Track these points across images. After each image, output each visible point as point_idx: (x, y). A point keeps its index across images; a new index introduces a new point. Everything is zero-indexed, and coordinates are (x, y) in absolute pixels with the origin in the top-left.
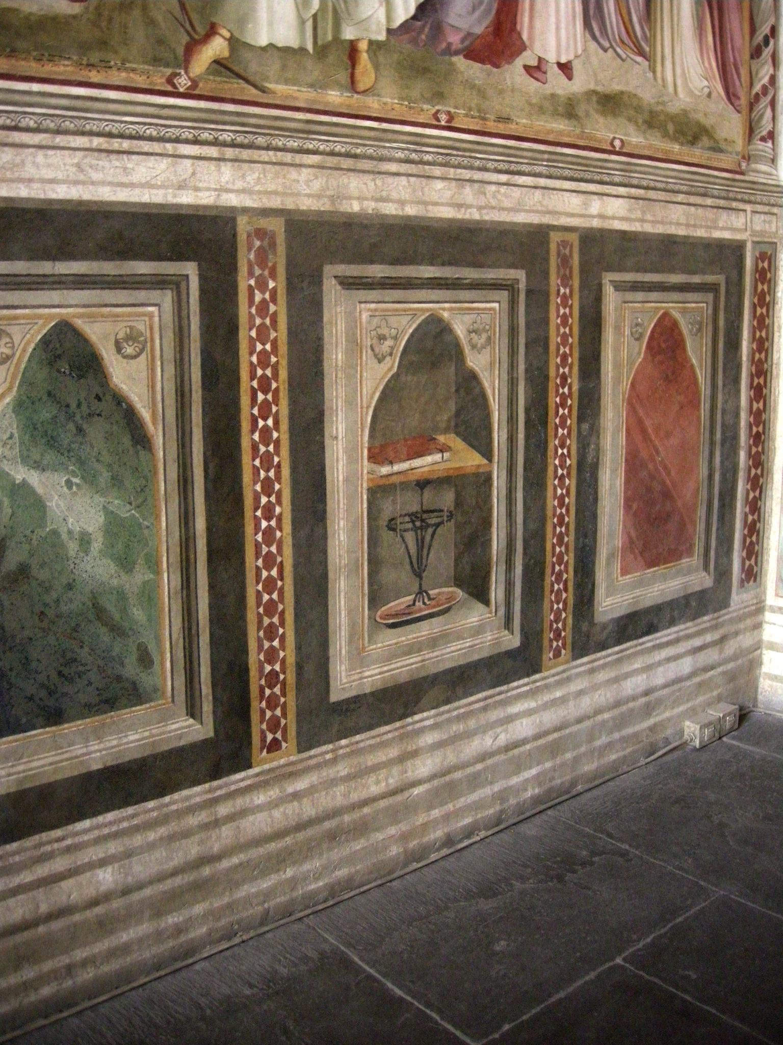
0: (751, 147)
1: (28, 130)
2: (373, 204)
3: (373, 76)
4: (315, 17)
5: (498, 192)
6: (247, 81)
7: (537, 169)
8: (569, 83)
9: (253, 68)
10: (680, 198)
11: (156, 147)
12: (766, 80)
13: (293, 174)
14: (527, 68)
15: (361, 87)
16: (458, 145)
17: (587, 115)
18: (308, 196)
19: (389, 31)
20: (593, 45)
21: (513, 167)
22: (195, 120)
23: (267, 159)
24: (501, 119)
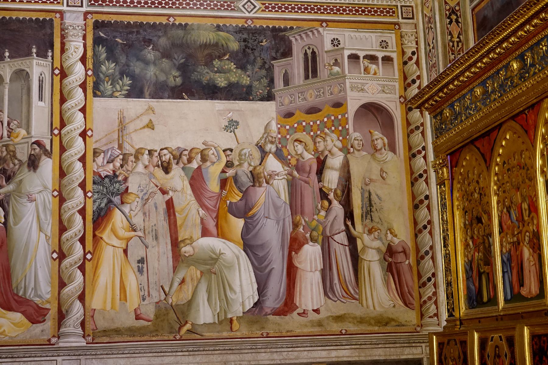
0: (423, 321)
4: (218, 313)
6: (197, 334)
7: (305, 345)
9: (199, 330)
11: (170, 354)
12: (430, 294)
13: (212, 357)
14: (298, 314)
15: (234, 330)
16: (271, 342)
17: (328, 324)
18: (217, 362)
19: (243, 313)
20: (329, 301)
21: (294, 346)
22: (182, 346)
23: (203, 353)
24: (288, 331)
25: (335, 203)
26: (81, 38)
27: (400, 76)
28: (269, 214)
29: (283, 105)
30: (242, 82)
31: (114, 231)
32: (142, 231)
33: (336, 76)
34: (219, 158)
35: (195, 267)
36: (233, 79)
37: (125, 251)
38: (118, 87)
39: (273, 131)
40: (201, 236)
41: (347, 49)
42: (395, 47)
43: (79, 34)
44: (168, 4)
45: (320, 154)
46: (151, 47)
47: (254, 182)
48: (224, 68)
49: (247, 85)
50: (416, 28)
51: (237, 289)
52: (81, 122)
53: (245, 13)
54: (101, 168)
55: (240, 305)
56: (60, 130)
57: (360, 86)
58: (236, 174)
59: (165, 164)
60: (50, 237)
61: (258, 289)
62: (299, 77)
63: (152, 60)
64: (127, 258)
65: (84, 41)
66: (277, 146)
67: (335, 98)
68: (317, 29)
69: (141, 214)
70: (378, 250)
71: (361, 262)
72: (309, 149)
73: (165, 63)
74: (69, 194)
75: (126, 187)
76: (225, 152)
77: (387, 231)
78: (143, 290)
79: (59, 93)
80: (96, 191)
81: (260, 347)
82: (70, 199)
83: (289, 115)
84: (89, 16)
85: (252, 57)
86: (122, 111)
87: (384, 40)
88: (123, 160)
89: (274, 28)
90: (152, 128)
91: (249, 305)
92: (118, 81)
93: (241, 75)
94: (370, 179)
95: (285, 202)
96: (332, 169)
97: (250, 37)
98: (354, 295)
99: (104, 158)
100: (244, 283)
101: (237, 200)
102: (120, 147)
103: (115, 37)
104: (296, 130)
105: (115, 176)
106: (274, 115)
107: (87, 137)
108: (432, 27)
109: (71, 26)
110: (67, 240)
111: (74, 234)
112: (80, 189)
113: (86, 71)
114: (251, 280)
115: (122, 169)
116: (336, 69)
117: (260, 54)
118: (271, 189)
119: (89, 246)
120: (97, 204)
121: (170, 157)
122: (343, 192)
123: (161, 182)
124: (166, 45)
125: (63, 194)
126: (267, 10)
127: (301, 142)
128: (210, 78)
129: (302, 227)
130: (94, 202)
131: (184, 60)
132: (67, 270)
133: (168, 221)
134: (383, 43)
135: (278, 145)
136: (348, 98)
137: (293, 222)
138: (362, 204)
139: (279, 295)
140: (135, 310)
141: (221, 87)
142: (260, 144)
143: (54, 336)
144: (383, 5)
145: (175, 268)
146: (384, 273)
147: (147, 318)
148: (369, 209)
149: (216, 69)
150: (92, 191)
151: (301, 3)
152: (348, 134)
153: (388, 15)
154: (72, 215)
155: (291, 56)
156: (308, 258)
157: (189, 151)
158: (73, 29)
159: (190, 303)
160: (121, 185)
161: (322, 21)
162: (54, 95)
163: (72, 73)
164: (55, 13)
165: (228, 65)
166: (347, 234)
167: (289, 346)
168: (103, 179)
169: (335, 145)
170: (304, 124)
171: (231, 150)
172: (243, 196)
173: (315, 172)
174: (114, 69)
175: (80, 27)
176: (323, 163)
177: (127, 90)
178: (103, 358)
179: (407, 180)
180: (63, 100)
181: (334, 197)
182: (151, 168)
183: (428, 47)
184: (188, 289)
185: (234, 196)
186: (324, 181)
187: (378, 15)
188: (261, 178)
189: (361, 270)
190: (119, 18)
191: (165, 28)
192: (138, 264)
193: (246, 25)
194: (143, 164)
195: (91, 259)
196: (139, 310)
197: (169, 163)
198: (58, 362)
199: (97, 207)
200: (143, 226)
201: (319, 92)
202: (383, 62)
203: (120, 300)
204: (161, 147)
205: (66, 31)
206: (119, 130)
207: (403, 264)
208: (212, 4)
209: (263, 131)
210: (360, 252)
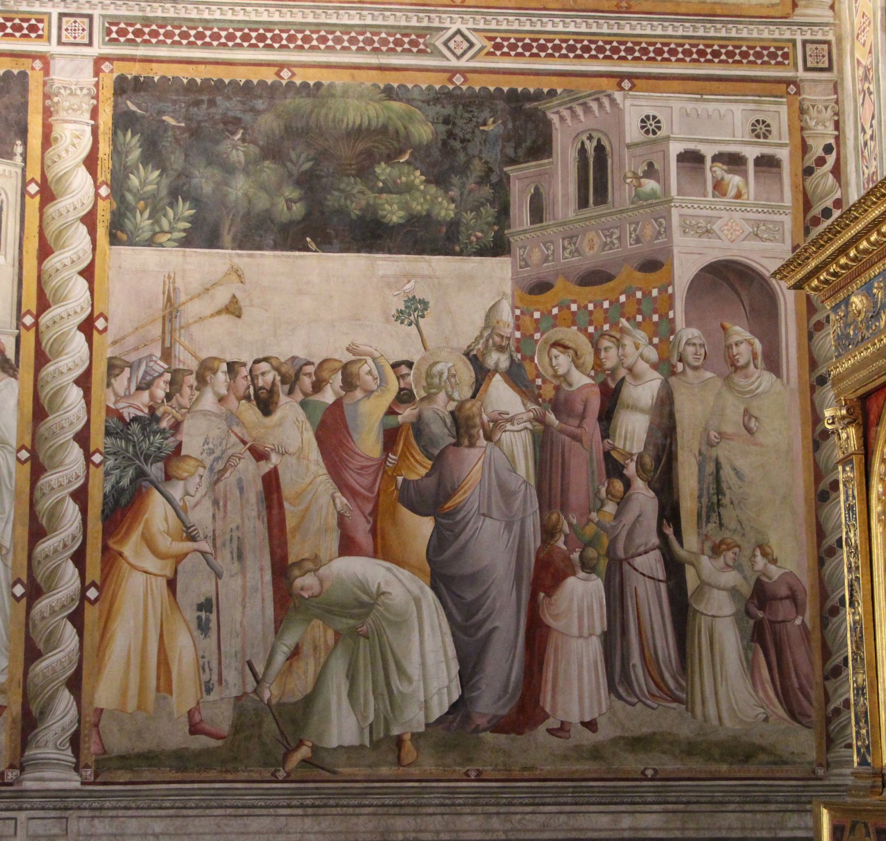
1: (191, 808)
2: (414, 835)
3: (415, 754)
4: (371, 726)
5: (524, 819)
8: (594, 735)
10: (731, 807)
11: (264, 811)
13: (354, 820)
14: (551, 731)
15: (406, 762)
17: (614, 754)
18: (364, 832)
19: (427, 725)
20: (619, 704)
21: (537, 801)
22: (289, 795)
24: (524, 769)
25: (639, 485)
26: (87, 117)
27: (795, 199)
28: (489, 507)
29: (527, 265)
30: (439, 214)
31: (148, 541)
32: (210, 541)
33: (650, 202)
34: (382, 380)
35: (324, 622)
36: (419, 207)
37: (172, 584)
38: (165, 223)
39: (504, 323)
40: (337, 554)
41: (676, 139)
42: (787, 136)
43: (84, 105)
44: (278, 40)
45: (608, 375)
46: (239, 136)
47: (458, 436)
48: (399, 181)
49: (448, 219)
50: (836, 92)
51: (414, 669)
52: (82, 299)
53: (448, 60)
54: (124, 400)
55: (421, 709)
56: (37, 317)
57: (702, 223)
58: (420, 417)
59: (263, 394)
60: (8, 551)
61: (461, 674)
62: (566, 204)
63: (240, 162)
64: (175, 599)
65: (92, 122)
66: (511, 356)
67: (645, 250)
68: (609, 96)
69: (207, 503)
70: (734, 592)
71: (694, 616)
72: (583, 364)
73: (269, 171)
74: (52, 457)
75: (177, 443)
76: (397, 369)
77: (754, 550)
78: (207, 670)
79: (37, 235)
80: (112, 450)
81: (461, 801)
82: (54, 468)
83: (541, 287)
84: (106, 67)
85: (462, 158)
86: (172, 275)
87: (761, 119)
88: (171, 383)
89: (513, 91)
90: (237, 313)
91: (439, 708)
92: (165, 209)
93: (436, 198)
94: (720, 433)
95: (526, 482)
96: (634, 408)
97: (459, 113)
98: (677, 693)
99: (130, 380)
100: (430, 658)
101: (418, 474)
102: (167, 355)
103: (161, 113)
104: (555, 322)
105: (154, 417)
106: (508, 288)
107: (95, 334)
108: (872, 89)
109: (65, 88)
110: (47, 556)
111: (61, 546)
112: (76, 446)
113: (97, 187)
114: (446, 655)
115: (170, 403)
116: (650, 185)
117: (481, 151)
118: (497, 452)
119: (94, 572)
120: (113, 479)
121: (274, 379)
122: (658, 459)
123: (254, 434)
124: (272, 130)
125: (41, 457)
126: (498, 53)
127: (566, 347)
128: (368, 204)
129: (563, 538)
130: (107, 474)
131: (310, 164)
132: (45, 622)
133: (266, 519)
134: (758, 127)
135: (514, 354)
136: (675, 251)
137: (541, 526)
138: (701, 489)
139: (506, 687)
140: (190, 713)
141: (391, 224)
142: (475, 352)
143: (12, 767)
144: (762, 40)
145: (280, 624)
146: (745, 643)
147: (213, 730)
148: (715, 500)
149: (381, 184)
150: (103, 451)
151: (575, 37)
152: (672, 331)
153: (773, 62)
154: (58, 502)
155: (550, 155)
156: (575, 607)
157: (316, 365)
158: (71, 94)
159: (309, 701)
160: (166, 439)
161: (621, 77)
162: (25, 239)
163: (65, 191)
164: (31, 60)
165: (408, 175)
166: (663, 555)
167: (526, 801)
168: (127, 425)
169: (641, 356)
170: (574, 307)
171: (410, 365)
172: (433, 466)
173: (597, 416)
174: (158, 184)
175: (85, 91)
176: (613, 395)
177: (185, 230)
178: (118, 817)
179: (804, 437)
180: (45, 251)
181: (637, 471)
182: (233, 403)
183: (861, 136)
184: (308, 668)
185: (415, 467)
186: (615, 436)
187: (750, 62)
188: (474, 427)
189: (693, 636)
190: (172, 71)
191: (272, 91)
192: (199, 613)
193: (451, 87)
194: (216, 393)
195: (97, 599)
196: (197, 713)
197: (272, 391)
198: (19, 823)
199: (113, 487)
200: (211, 528)
201: (611, 237)
202: (759, 169)
203: (158, 689)
204: (256, 357)
205: (56, 99)
206: (164, 318)
207: (789, 625)
208: (376, 38)
209: (481, 323)
210: (692, 595)
